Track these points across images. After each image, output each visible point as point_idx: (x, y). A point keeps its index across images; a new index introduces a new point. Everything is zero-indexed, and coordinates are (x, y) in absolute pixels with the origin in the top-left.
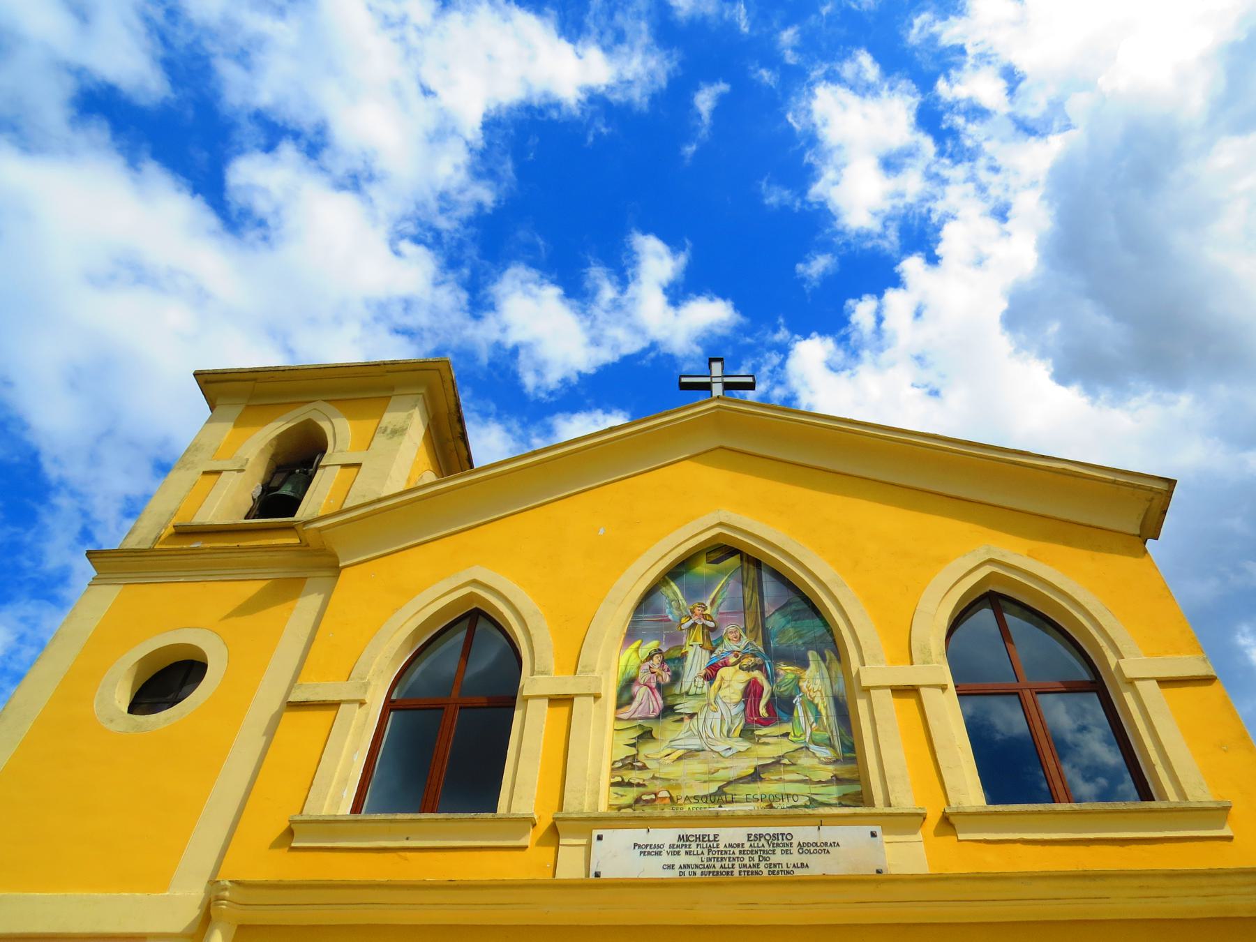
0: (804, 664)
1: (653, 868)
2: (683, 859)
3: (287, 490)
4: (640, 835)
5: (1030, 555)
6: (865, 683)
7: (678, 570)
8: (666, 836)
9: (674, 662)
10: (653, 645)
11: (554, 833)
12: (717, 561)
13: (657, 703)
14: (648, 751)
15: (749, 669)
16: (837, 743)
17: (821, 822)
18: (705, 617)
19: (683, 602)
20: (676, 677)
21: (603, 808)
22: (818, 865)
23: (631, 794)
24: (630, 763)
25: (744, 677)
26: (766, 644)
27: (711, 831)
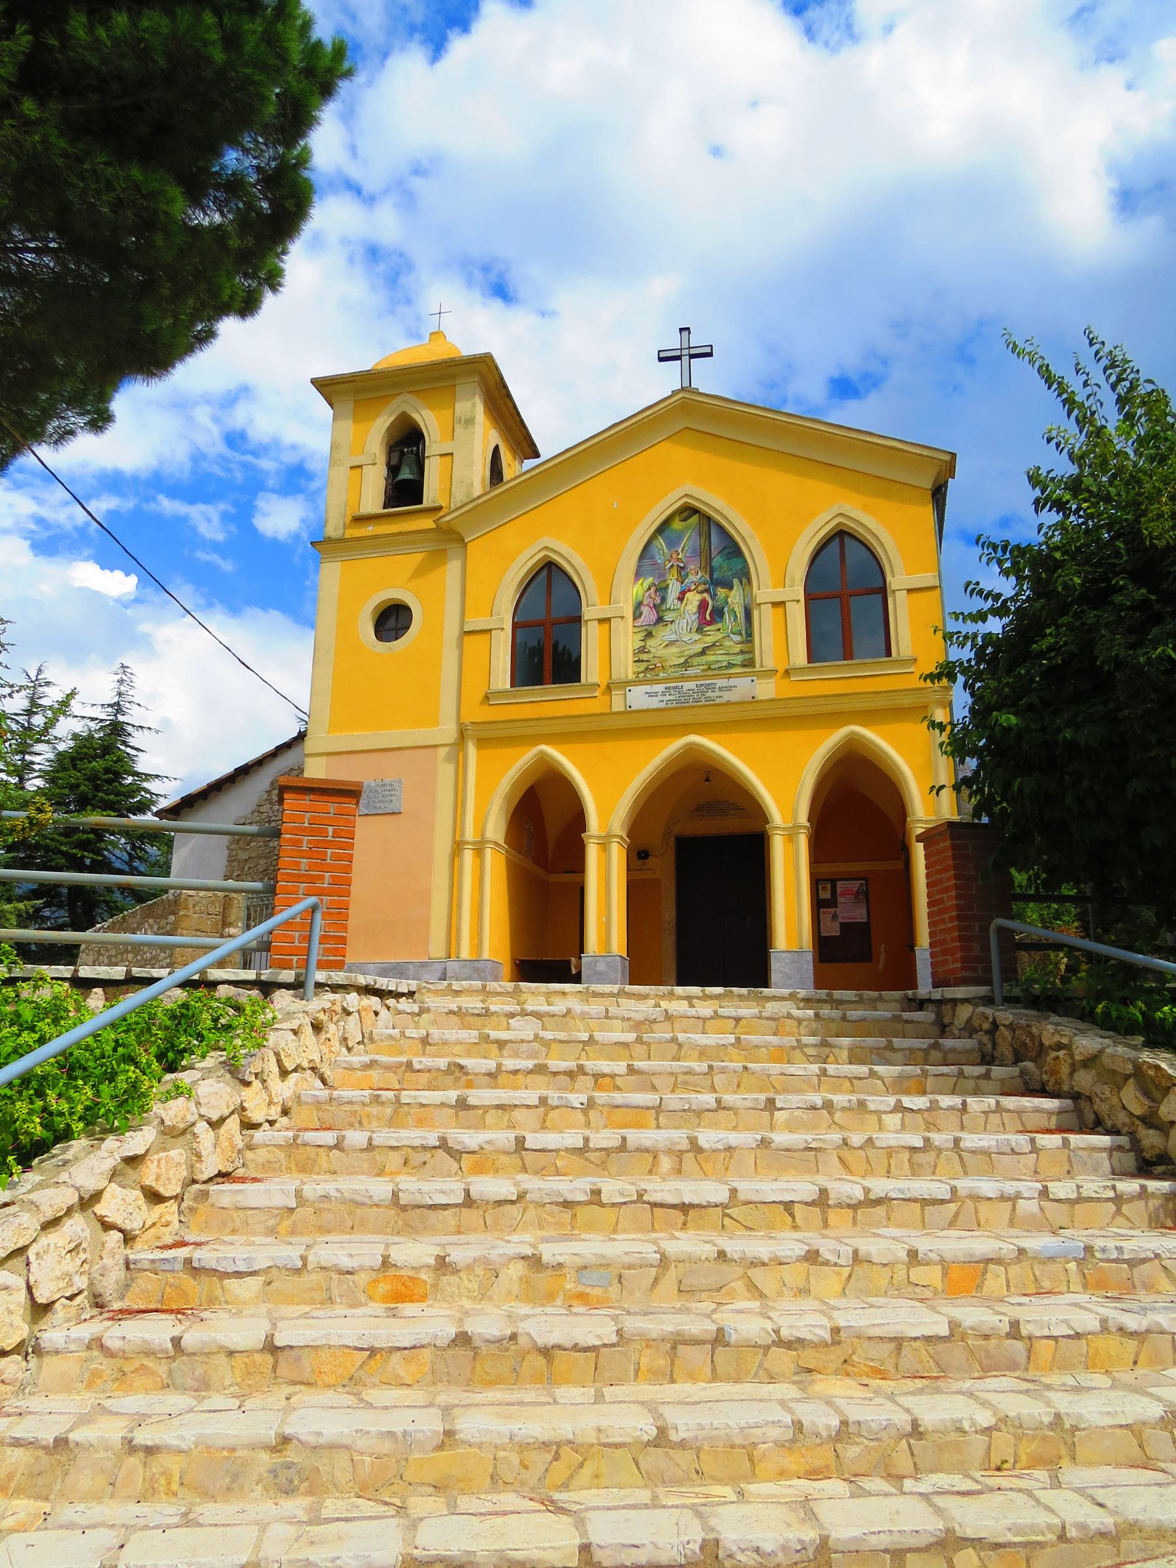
0: (730, 587)
1: (654, 703)
2: (668, 697)
3: (406, 474)
4: (647, 688)
5: (865, 509)
6: (758, 601)
7: (662, 529)
8: (660, 688)
9: (662, 590)
10: (650, 580)
11: (609, 689)
12: (685, 520)
13: (653, 616)
14: (651, 643)
15: (701, 592)
16: (744, 632)
17: (730, 677)
18: (678, 560)
19: (666, 550)
20: (663, 600)
21: (631, 676)
22: (727, 696)
23: (644, 665)
24: (642, 650)
25: (699, 597)
26: (711, 578)
27: (680, 684)
